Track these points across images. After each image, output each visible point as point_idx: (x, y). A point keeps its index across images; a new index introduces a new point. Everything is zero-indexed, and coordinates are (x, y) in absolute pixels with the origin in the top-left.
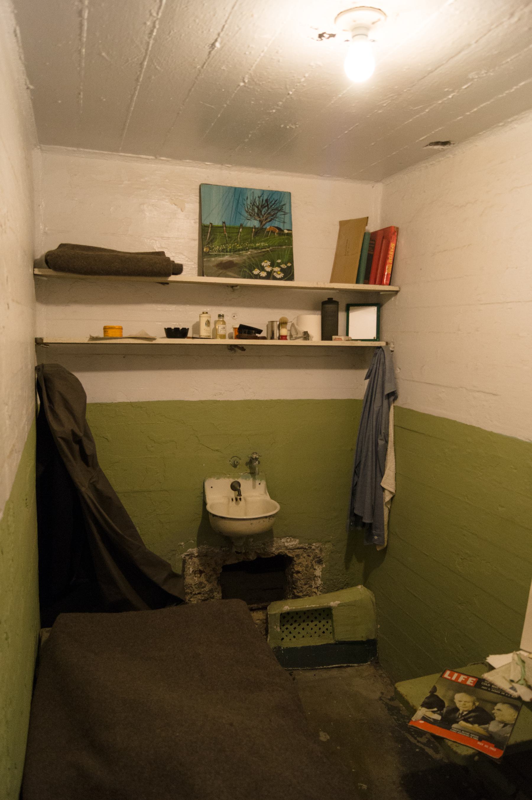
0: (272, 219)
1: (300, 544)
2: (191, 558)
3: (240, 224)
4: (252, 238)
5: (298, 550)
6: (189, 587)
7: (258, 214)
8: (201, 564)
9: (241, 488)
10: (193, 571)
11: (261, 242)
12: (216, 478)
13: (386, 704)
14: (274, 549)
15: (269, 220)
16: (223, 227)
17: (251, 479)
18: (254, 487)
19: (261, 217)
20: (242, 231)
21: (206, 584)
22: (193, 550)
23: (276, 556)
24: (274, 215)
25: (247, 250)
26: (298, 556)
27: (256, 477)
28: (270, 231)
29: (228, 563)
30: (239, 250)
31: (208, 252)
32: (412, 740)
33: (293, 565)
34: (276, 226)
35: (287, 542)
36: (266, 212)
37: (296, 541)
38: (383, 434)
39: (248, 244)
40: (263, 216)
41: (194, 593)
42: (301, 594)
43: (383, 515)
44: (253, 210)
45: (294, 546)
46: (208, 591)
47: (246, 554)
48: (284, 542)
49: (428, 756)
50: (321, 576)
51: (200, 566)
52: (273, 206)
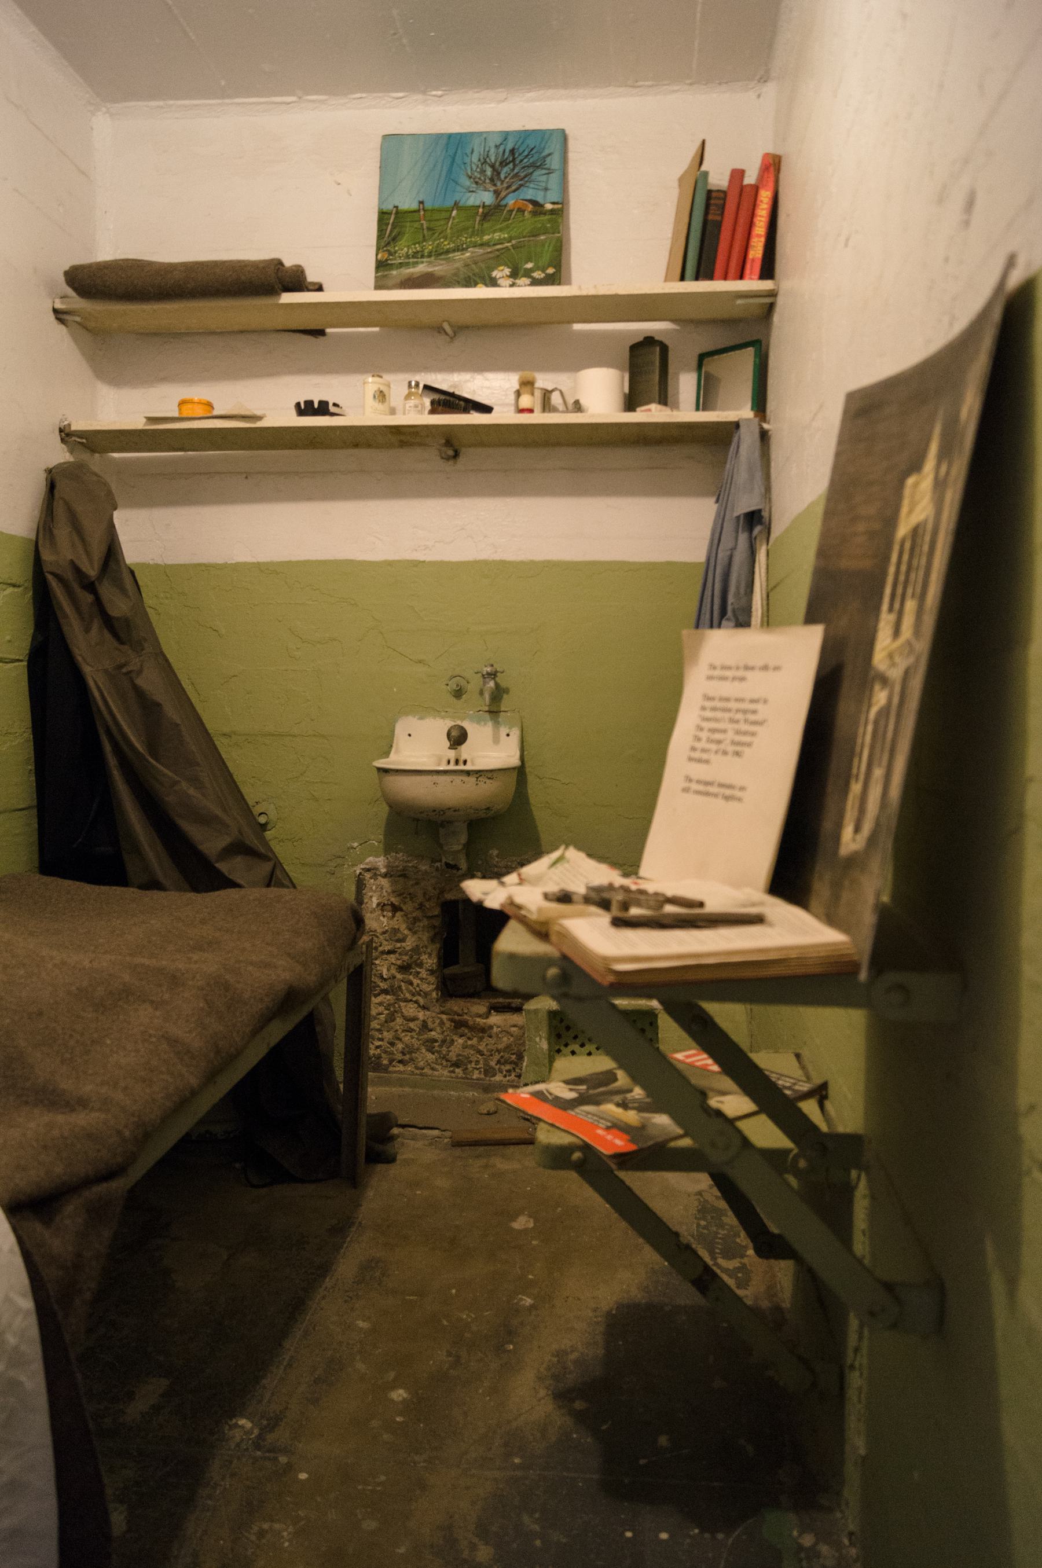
0: (521, 186)
2: (375, 876)
3: (453, 203)
4: (477, 226)
7: (492, 180)
8: (393, 892)
10: (378, 904)
11: (494, 232)
15: (514, 188)
16: (418, 211)
17: (490, 724)
18: (496, 740)
19: (499, 184)
20: (457, 214)
21: (407, 936)
22: (377, 859)
24: (525, 177)
25: (463, 249)
28: (516, 210)
30: (448, 252)
31: (387, 260)
34: (529, 197)
36: (509, 174)
39: (466, 238)
40: (502, 184)
44: (483, 172)
46: (410, 950)
52: (525, 160)
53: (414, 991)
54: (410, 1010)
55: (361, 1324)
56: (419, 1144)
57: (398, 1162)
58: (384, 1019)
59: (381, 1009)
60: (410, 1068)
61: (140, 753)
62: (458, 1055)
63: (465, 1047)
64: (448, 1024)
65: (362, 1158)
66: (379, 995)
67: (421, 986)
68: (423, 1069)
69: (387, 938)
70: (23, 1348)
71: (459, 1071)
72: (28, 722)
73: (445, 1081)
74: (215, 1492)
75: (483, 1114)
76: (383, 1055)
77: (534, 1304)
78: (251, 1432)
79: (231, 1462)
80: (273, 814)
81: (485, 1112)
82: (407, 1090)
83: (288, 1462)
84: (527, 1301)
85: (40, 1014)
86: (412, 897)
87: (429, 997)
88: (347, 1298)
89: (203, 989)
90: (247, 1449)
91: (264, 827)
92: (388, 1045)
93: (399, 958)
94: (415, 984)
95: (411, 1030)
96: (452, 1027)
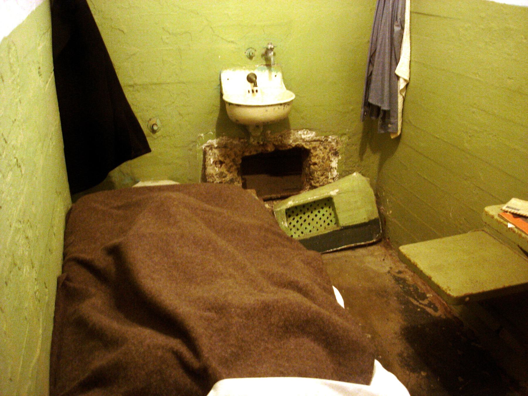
1: (316, 136)
5: (315, 143)
8: (220, 155)
9: (258, 81)
10: (213, 162)
12: (232, 69)
13: (394, 276)
14: (291, 141)
23: (293, 148)
26: (314, 148)
27: (272, 69)
29: (247, 154)
32: (415, 303)
33: (310, 157)
35: (304, 134)
37: (312, 133)
38: (399, 21)
42: (317, 185)
43: (397, 103)
45: (310, 138)
46: (229, 181)
47: (264, 145)
48: (300, 135)
49: (428, 313)
50: (337, 167)
51: (220, 156)
86: (229, 156)
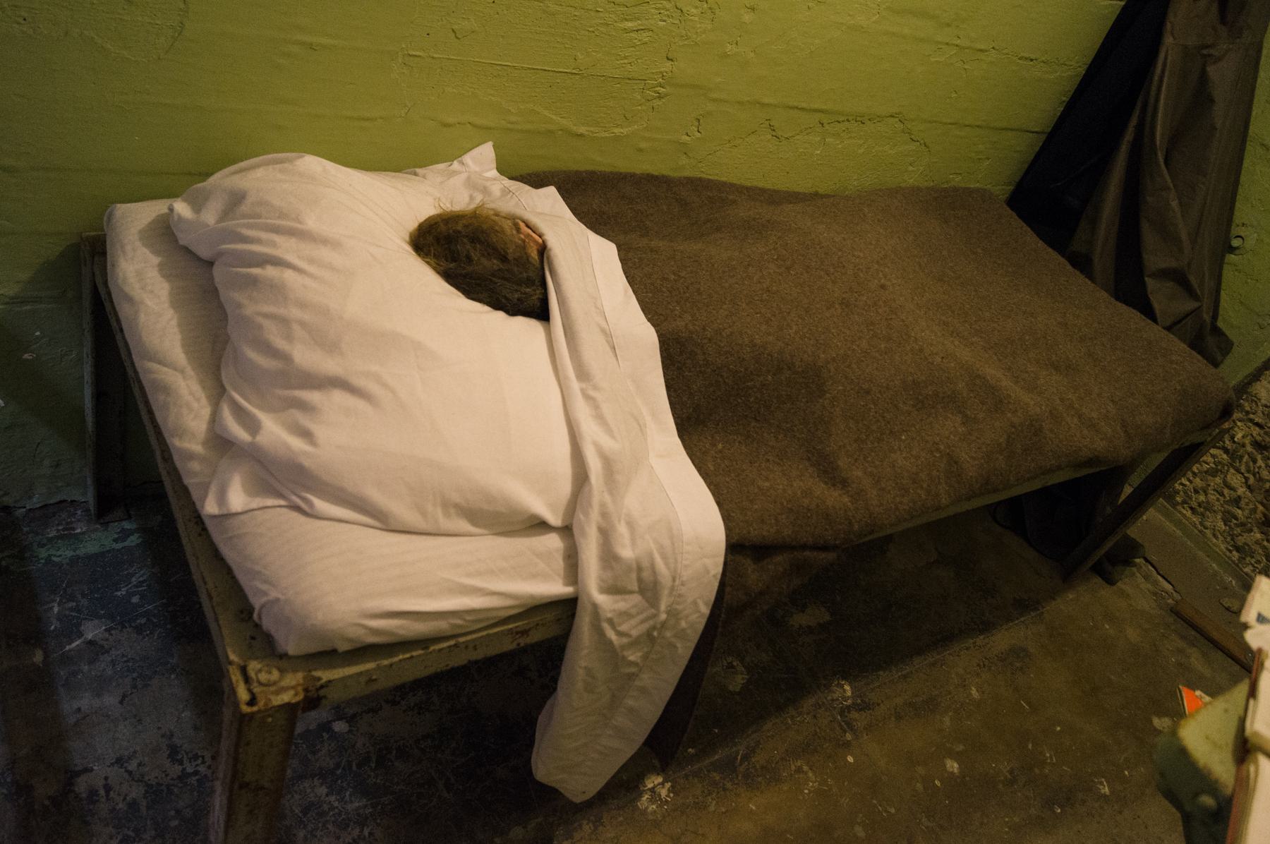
6: (1252, 401)
41: (1251, 416)
53: (1252, 469)
54: (1235, 480)
55: (974, 691)
56: (1145, 586)
57: (1115, 587)
58: (1205, 469)
59: (1210, 459)
60: (1195, 519)
61: (1155, 145)
62: (1246, 544)
63: (1257, 542)
64: (1259, 515)
65: (1090, 563)
66: (1219, 448)
67: (1261, 470)
68: (1206, 528)
69: (1266, 413)
70: (689, 631)
71: (1236, 555)
72: (1091, 55)
73: (1217, 552)
74: (797, 717)
75: (1223, 606)
76: (1181, 493)
77: (1108, 796)
78: (846, 699)
79: (820, 708)
80: (1250, 242)
81: (1227, 606)
82: (1179, 533)
83: (849, 741)
84: (1104, 789)
85: (868, 392)
87: (1261, 484)
88: (982, 664)
89: (1014, 427)
90: (835, 708)
91: (1232, 250)
92: (1192, 490)
93: (1262, 435)
94: (1258, 465)
95: (1222, 494)
96: (1261, 521)
